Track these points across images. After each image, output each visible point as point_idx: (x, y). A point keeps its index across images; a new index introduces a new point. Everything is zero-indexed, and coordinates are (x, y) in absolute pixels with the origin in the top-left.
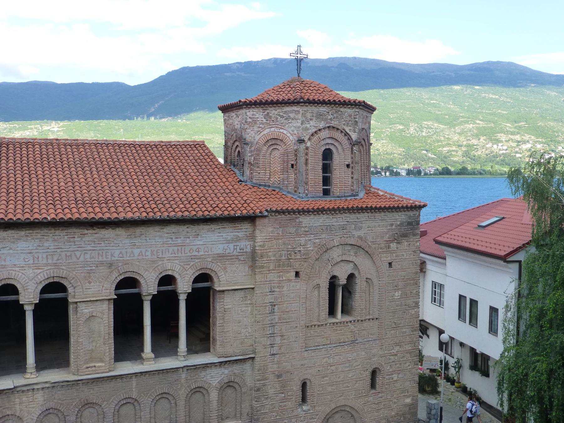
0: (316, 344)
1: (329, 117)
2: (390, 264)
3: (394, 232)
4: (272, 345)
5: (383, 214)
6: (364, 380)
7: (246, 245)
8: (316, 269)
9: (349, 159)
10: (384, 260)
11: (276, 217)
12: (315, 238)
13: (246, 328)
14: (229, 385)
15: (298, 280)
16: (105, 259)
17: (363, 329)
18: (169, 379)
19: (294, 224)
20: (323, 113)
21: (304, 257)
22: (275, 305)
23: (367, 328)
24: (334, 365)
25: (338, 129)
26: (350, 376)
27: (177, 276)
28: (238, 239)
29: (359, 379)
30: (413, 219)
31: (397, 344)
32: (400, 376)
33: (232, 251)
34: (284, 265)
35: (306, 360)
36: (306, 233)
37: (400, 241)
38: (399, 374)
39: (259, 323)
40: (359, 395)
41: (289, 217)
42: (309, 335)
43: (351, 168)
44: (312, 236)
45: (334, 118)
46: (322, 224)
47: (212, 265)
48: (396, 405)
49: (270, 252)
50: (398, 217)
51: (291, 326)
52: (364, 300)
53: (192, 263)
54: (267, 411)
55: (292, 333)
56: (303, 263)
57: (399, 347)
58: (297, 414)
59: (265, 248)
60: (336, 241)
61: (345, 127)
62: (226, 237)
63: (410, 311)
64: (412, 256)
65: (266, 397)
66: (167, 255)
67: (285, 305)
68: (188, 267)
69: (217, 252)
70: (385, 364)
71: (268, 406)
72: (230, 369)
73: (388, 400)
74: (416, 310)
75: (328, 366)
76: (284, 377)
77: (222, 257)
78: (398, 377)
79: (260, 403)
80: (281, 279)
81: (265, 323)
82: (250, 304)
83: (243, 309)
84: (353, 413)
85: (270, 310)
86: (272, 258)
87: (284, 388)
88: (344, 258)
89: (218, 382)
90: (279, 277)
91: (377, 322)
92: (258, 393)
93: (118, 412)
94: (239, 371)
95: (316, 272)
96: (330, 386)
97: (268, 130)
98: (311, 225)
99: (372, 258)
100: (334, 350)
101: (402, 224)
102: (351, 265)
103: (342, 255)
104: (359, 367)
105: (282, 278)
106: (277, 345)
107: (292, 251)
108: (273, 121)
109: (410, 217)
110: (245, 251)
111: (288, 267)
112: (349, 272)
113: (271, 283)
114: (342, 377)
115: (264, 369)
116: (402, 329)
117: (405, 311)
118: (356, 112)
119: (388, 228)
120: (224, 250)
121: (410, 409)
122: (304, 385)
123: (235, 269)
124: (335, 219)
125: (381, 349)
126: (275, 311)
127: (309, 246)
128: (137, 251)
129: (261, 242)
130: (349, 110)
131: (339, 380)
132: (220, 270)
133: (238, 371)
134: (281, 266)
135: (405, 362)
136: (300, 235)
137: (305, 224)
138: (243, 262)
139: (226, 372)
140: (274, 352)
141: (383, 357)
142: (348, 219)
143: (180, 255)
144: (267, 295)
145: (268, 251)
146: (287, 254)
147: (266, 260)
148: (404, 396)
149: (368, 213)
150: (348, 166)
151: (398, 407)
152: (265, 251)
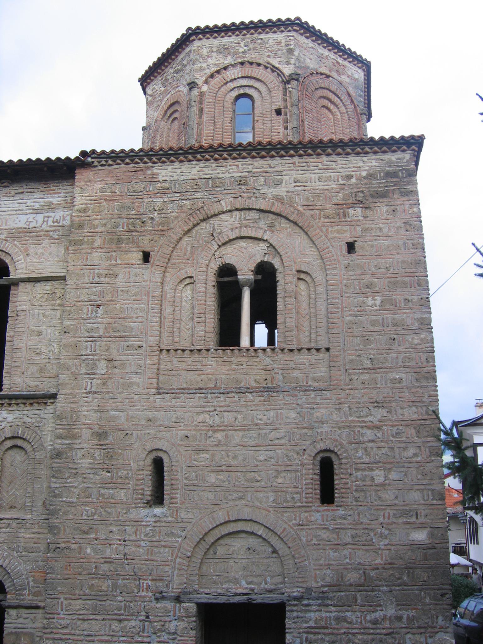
0: (185, 386)
1: (241, 50)
2: (351, 247)
3: (356, 190)
5: (325, 159)
9: (279, 102)
13: (50, 345)
15: (148, 265)
17: (294, 366)
19: (142, 177)
20: (229, 46)
21: (160, 228)
22: (98, 306)
23: (302, 367)
24: (222, 430)
25: (259, 65)
26: (261, 458)
28: (51, 207)
29: (283, 468)
30: (398, 166)
31: (378, 404)
32: (393, 475)
33: (39, 224)
35: (158, 411)
36: (165, 191)
37: (371, 205)
38: (390, 470)
39: (67, 334)
41: (134, 167)
42: (169, 366)
43: (283, 114)
44: (178, 195)
45: (249, 50)
46: (196, 177)
47: (6, 244)
48: (386, 542)
49: (95, 219)
50: (361, 164)
51: (128, 344)
52: (294, 311)
54: (75, 500)
56: (156, 238)
57: (385, 410)
59: (88, 214)
60: (226, 203)
61: (270, 60)
62: (33, 204)
63: (409, 338)
64: (402, 232)
67: (118, 306)
69: (16, 226)
70: (350, 443)
72: (17, 414)
73: (363, 526)
74: (422, 336)
75: (208, 430)
76: (111, 439)
78: (386, 477)
79: (60, 481)
80: (113, 262)
81: (78, 335)
82: (59, 305)
83: (47, 313)
84: (274, 540)
85: (90, 312)
86: (99, 230)
87: (110, 459)
88: (244, 232)
90: (110, 259)
91: (323, 355)
92: (58, 461)
94: (34, 420)
96: (212, 471)
97: (166, 99)
98: (175, 178)
99: (307, 233)
100: (222, 399)
101: (371, 176)
102: (263, 246)
103: (240, 228)
104: (282, 441)
105: (116, 261)
106: (100, 376)
107: (137, 219)
108: (170, 83)
109: (389, 163)
110: (61, 224)
112: (258, 259)
113: (95, 269)
114: (241, 458)
115: (72, 417)
116: (391, 372)
117: (395, 336)
118: (289, 36)
120: (28, 223)
121: (426, 557)
123: (41, 251)
124: (223, 169)
125: (339, 410)
127: (170, 211)
129: (82, 204)
130: (275, 36)
132: (17, 252)
133: (30, 420)
135: (403, 445)
136: (154, 195)
137: (163, 177)
138: (57, 241)
139: (10, 418)
140: (93, 389)
141: (344, 427)
144: (84, 288)
145: (93, 218)
146: (127, 223)
147: (88, 232)
148: (407, 523)
149: (292, 156)
150: (278, 112)
151: (393, 548)
152: (87, 218)
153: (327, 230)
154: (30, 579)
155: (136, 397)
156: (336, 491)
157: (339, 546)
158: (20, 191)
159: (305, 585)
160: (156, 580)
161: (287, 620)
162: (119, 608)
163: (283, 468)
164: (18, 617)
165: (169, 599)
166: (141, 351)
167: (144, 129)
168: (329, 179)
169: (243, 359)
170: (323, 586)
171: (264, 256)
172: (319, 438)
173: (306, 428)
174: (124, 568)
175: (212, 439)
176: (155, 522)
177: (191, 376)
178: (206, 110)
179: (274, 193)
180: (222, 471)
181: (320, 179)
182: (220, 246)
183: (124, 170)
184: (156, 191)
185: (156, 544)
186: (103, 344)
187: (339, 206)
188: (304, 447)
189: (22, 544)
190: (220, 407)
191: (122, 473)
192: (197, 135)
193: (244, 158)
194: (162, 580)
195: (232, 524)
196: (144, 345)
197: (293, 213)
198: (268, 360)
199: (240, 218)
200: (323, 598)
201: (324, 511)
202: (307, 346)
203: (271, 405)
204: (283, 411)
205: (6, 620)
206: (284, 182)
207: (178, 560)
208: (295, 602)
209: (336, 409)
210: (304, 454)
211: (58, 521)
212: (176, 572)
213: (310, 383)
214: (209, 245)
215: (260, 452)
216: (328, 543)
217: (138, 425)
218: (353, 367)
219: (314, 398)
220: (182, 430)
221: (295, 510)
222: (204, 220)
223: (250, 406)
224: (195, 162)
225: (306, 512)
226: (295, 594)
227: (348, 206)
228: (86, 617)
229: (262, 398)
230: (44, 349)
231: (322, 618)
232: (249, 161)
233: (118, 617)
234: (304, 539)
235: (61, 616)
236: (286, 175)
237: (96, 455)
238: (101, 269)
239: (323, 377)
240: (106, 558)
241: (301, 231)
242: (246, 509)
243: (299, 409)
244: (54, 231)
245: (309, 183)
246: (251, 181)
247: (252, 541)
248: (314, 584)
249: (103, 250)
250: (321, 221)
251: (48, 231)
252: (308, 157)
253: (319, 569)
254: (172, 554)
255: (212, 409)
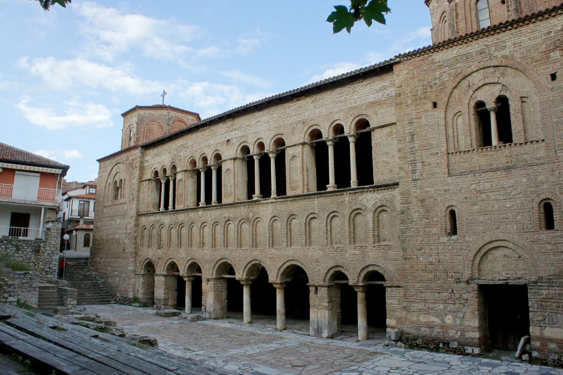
0: (463, 171)
2: (553, 77)
4: (414, 172)
5: (531, 25)
6: (530, 211)
7: (392, 91)
8: (456, 97)
10: (542, 73)
11: (410, 61)
12: (451, 69)
14: (381, 209)
15: (436, 109)
16: (301, 119)
18: (337, 201)
21: (440, 88)
22: (414, 135)
23: (528, 152)
24: (484, 193)
26: (508, 206)
27: (343, 124)
28: (385, 88)
29: (521, 211)
33: (380, 98)
34: (420, 99)
35: (450, 186)
36: (440, 67)
40: (524, 231)
42: (454, 161)
44: (447, 68)
46: (456, 55)
51: (431, 152)
53: (352, 112)
54: (413, 234)
55: (433, 159)
58: (443, 241)
60: (474, 66)
65: (411, 220)
66: (336, 110)
67: (424, 134)
68: (349, 115)
71: (413, 229)
76: (427, 202)
77: (372, 104)
80: (419, 111)
82: (395, 138)
83: (390, 143)
86: (409, 95)
88: (487, 81)
89: (373, 205)
90: (416, 109)
92: (403, 216)
93: (309, 223)
95: (456, 100)
97: (439, 11)
98: (445, 58)
100: (483, 176)
102: (499, 87)
103: (484, 79)
106: (419, 171)
111: (424, 100)
112: (497, 94)
114: (496, 207)
119: (544, 37)
122: (453, 214)
123: (383, 111)
124: (470, 47)
125: (552, 175)
126: (415, 140)
128: (317, 111)
131: (494, 209)
134: (418, 99)
139: (379, 196)
142: (486, 43)
143: (343, 108)
149: (510, 30)
152: (402, 90)
153: (537, 69)
154: (396, 274)
155: (438, 179)
156: (555, 222)
157: (558, 253)
158: (369, 83)
159: (538, 275)
160: (456, 273)
161: (529, 294)
162: (439, 287)
163: (521, 211)
164: (392, 291)
165: (463, 282)
166: (439, 155)
167: (431, 30)
168: (536, 38)
169: (493, 152)
170: (549, 276)
171: (500, 92)
172: (542, 192)
173: (533, 187)
174: (439, 267)
175: (479, 198)
176: (454, 243)
177: (466, 165)
178: (460, 13)
179: (502, 55)
180: (486, 214)
181: (530, 39)
182: (474, 92)
183: (417, 61)
184: (436, 68)
185: (454, 254)
186: (419, 154)
187: (544, 53)
188: (533, 198)
189: (391, 257)
190: (483, 180)
191: (435, 219)
192: (457, 29)
193: (482, 38)
194: (459, 272)
195: (495, 243)
196: (439, 152)
197: (514, 64)
198: (508, 151)
199: (483, 73)
200: (549, 283)
201: (547, 233)
202: (531, 140)
203: (511, 176)
204: (518, 179)
205: (386, 293)
206: (507, 46)
207: (467, 262)
208: (533, 284)
209: (551, 175)
210: (533, 202)
211: (406, 245)
212: (466, 268)
213: (534, 161)
214: (468, 92)
215: (507, 203)
216: (551, 251)
217: (440, 194)
218: (560, 148)
219: (537, 169)
220: (463, 194)
221: (529, 233)
222: (464, 79)
223: (500, 178)
224: (454, 47)
225: (537, 234)
226: (533, 280)
227: (550, 51)
228: (423, 291)
229: (506, 173)
230: (391, 161)
231: (550, 293)
232: (485, 39)
233: (438, 291)
234: (536, 250)
235: (411, 291)
236: (508, 42)
237: (421, 211)
238: (413, 115)
239: (542, 157)
240: (430, 262)
241: (521, 73)
242: (501, 234)
243: (528, 177)
244: (388, 100)
245: (523, 43)
246: (487, 51)
247: (506, 251)
248: (544, 275)
249: (413, 105)
250: (532, 65)
251: (385, 100)
252: (520, 28)
253: (546, 266)
254: (463, 259)
255: (479, 181)
